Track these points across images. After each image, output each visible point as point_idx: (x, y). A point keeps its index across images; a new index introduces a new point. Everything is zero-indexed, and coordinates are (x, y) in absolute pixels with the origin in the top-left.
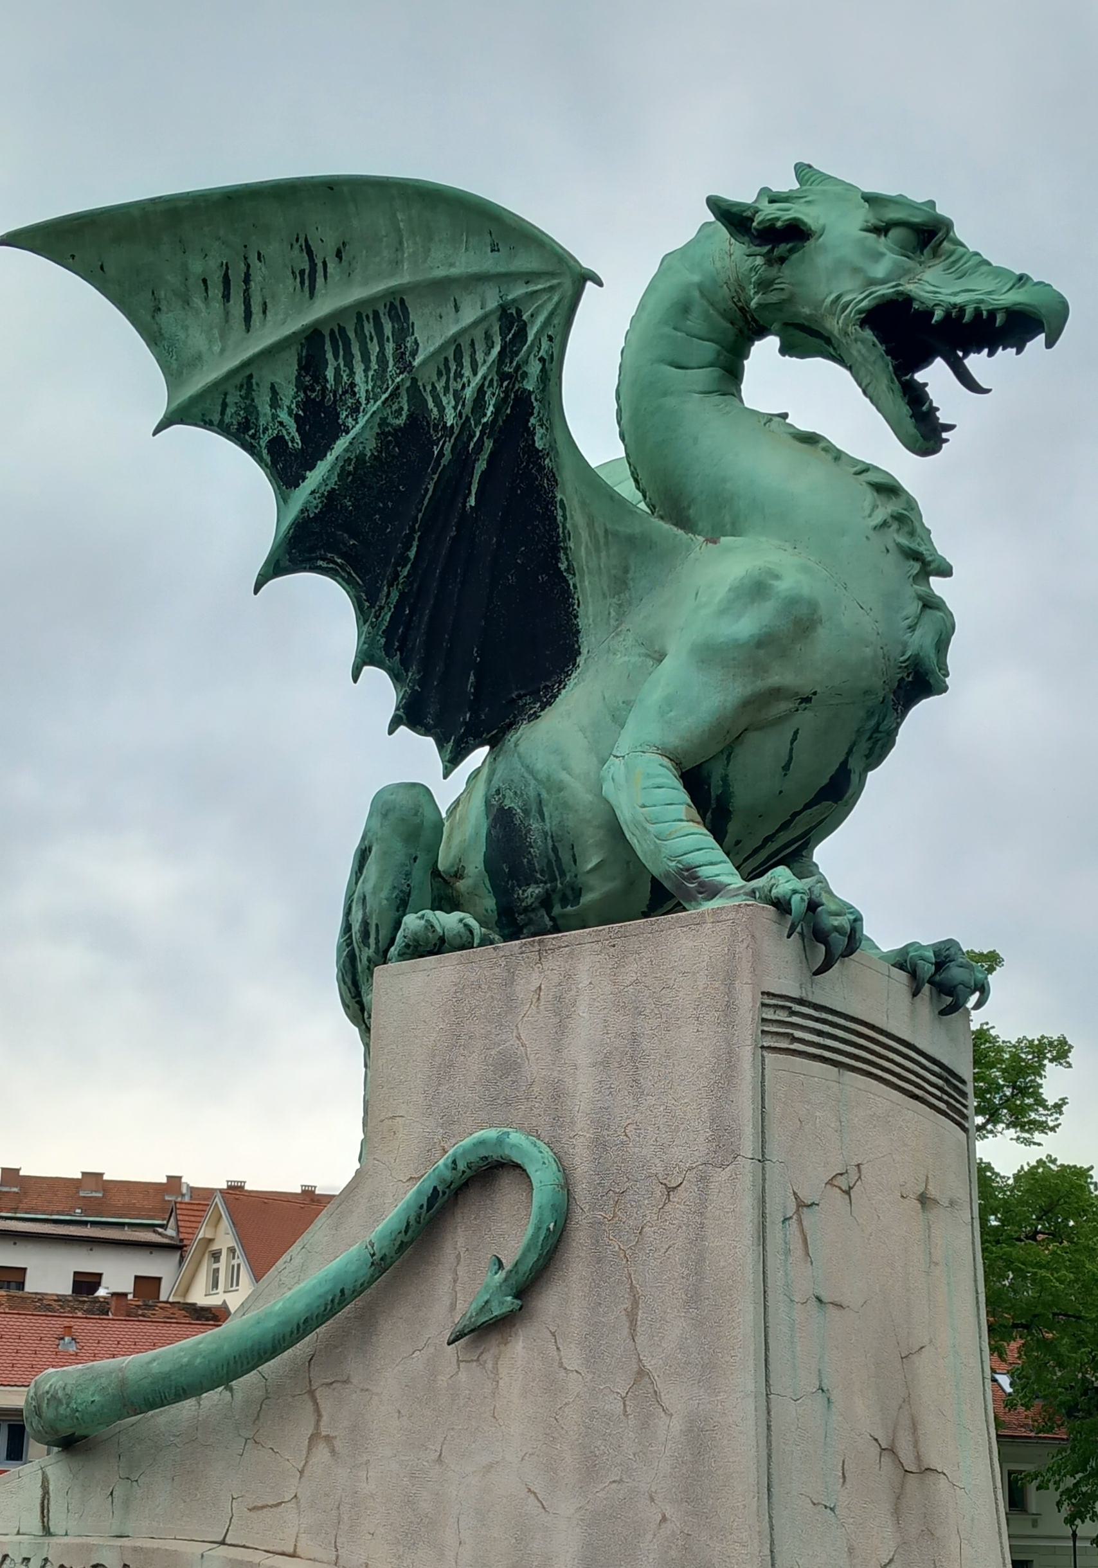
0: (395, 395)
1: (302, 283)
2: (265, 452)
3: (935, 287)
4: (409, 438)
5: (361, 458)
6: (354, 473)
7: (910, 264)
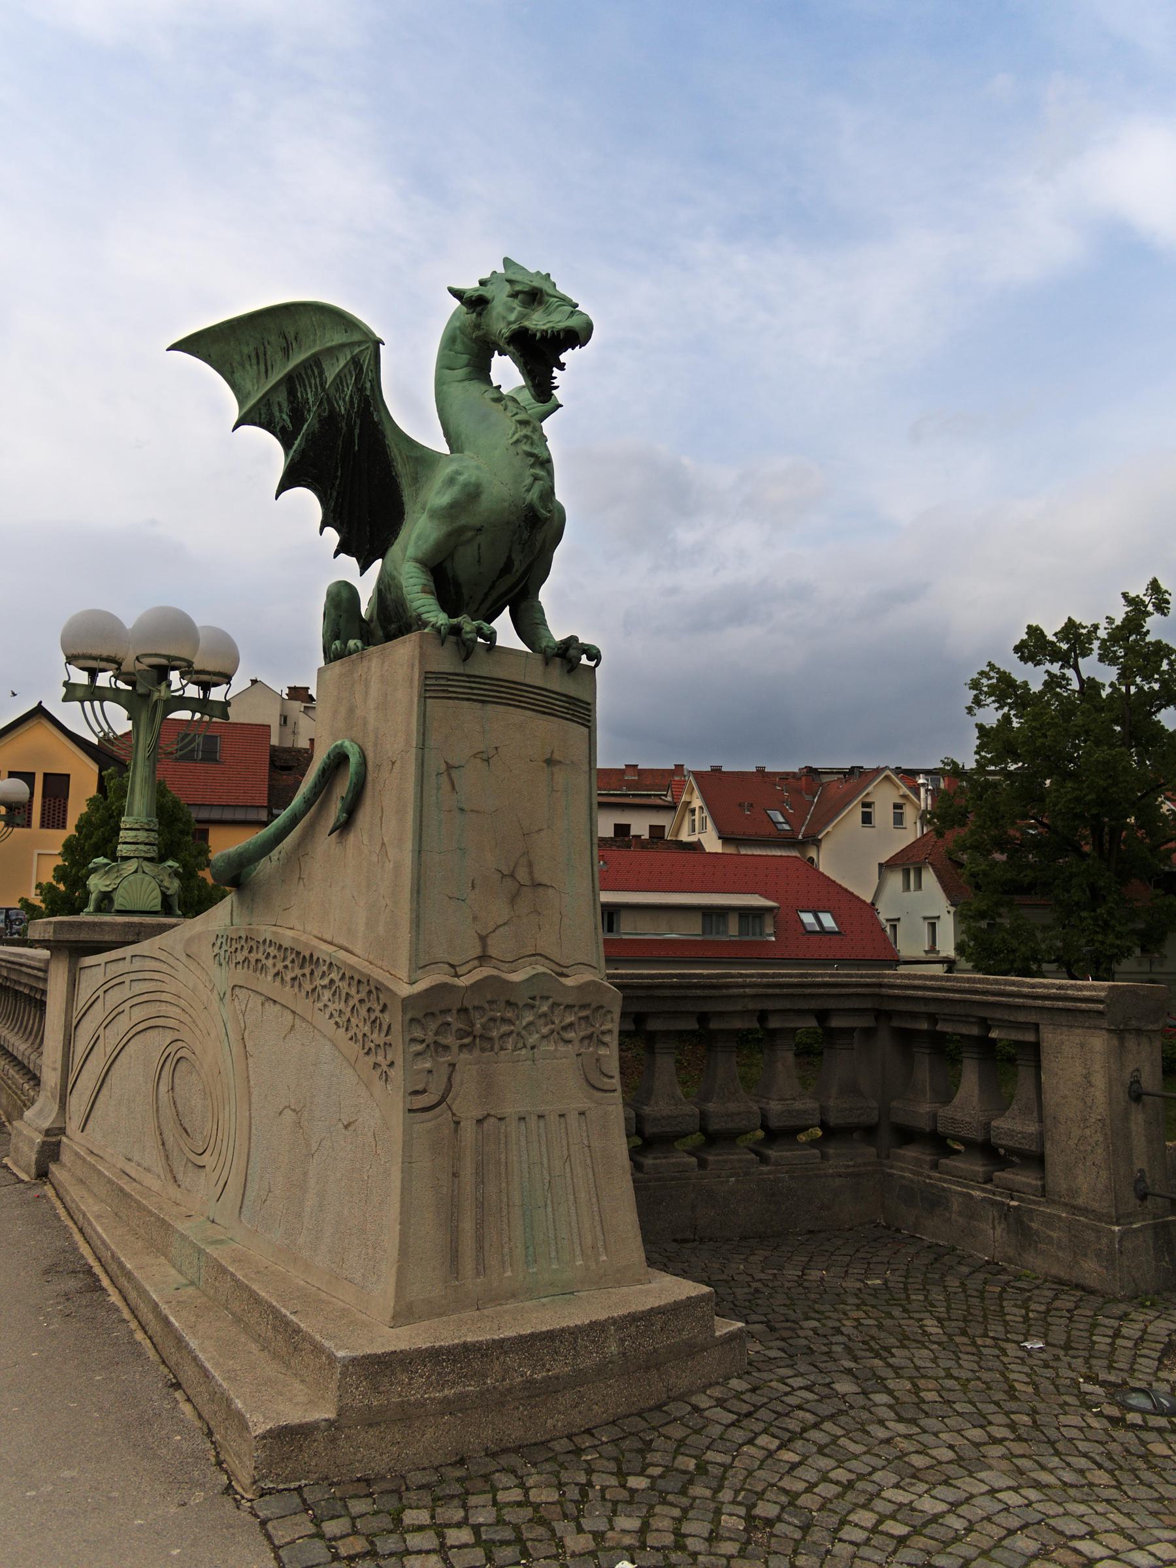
0: (321, 403)
3: (539, 321)
4: (330, 421)
5: (313, 433)
6: (311, 439)
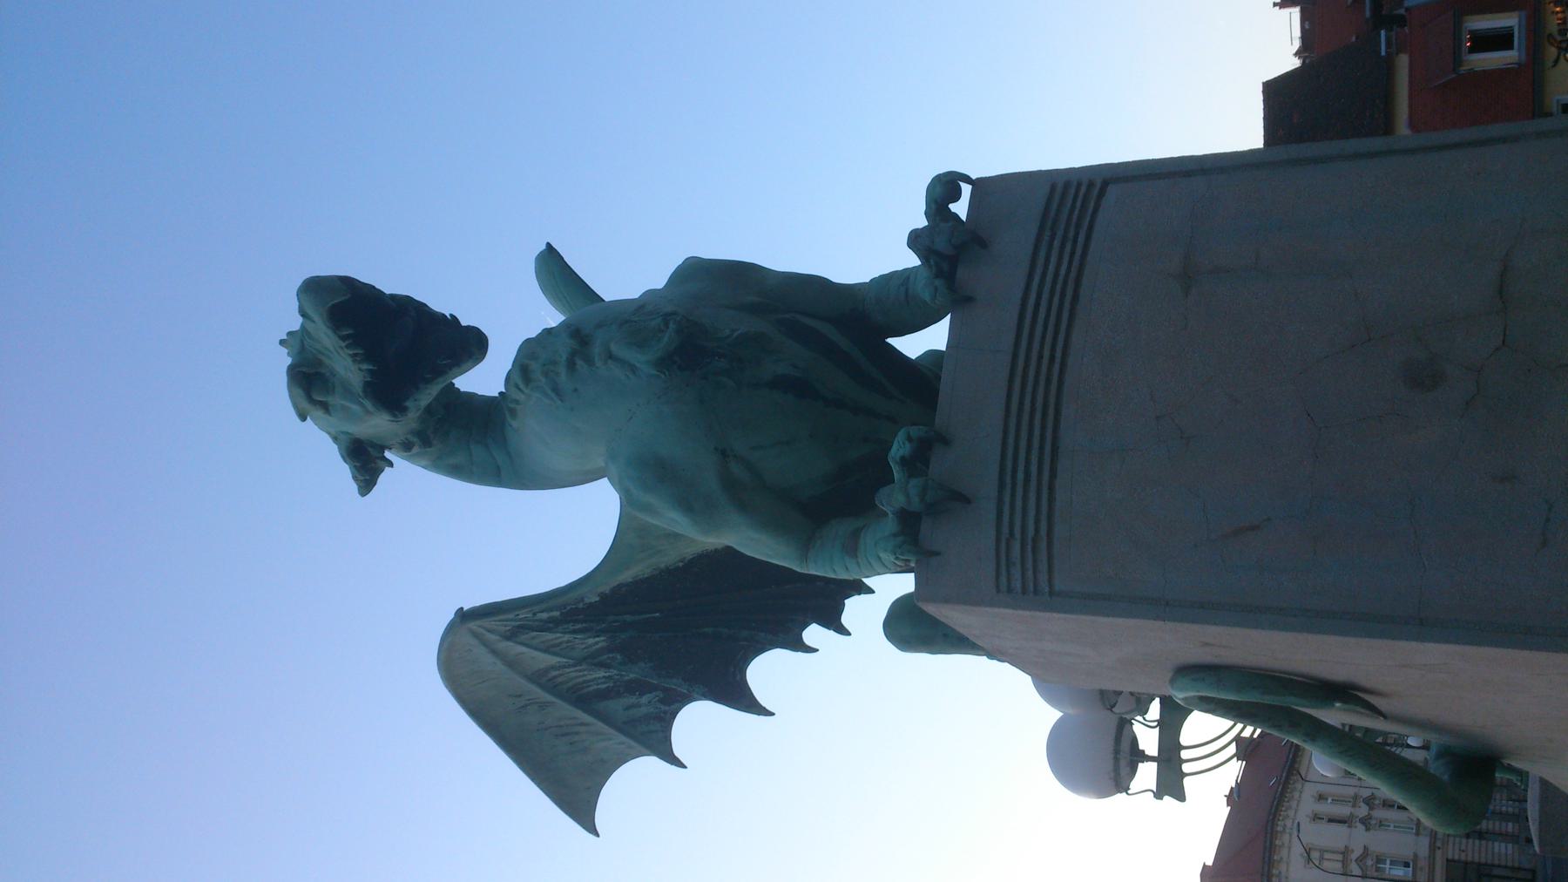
3: (346, 367)
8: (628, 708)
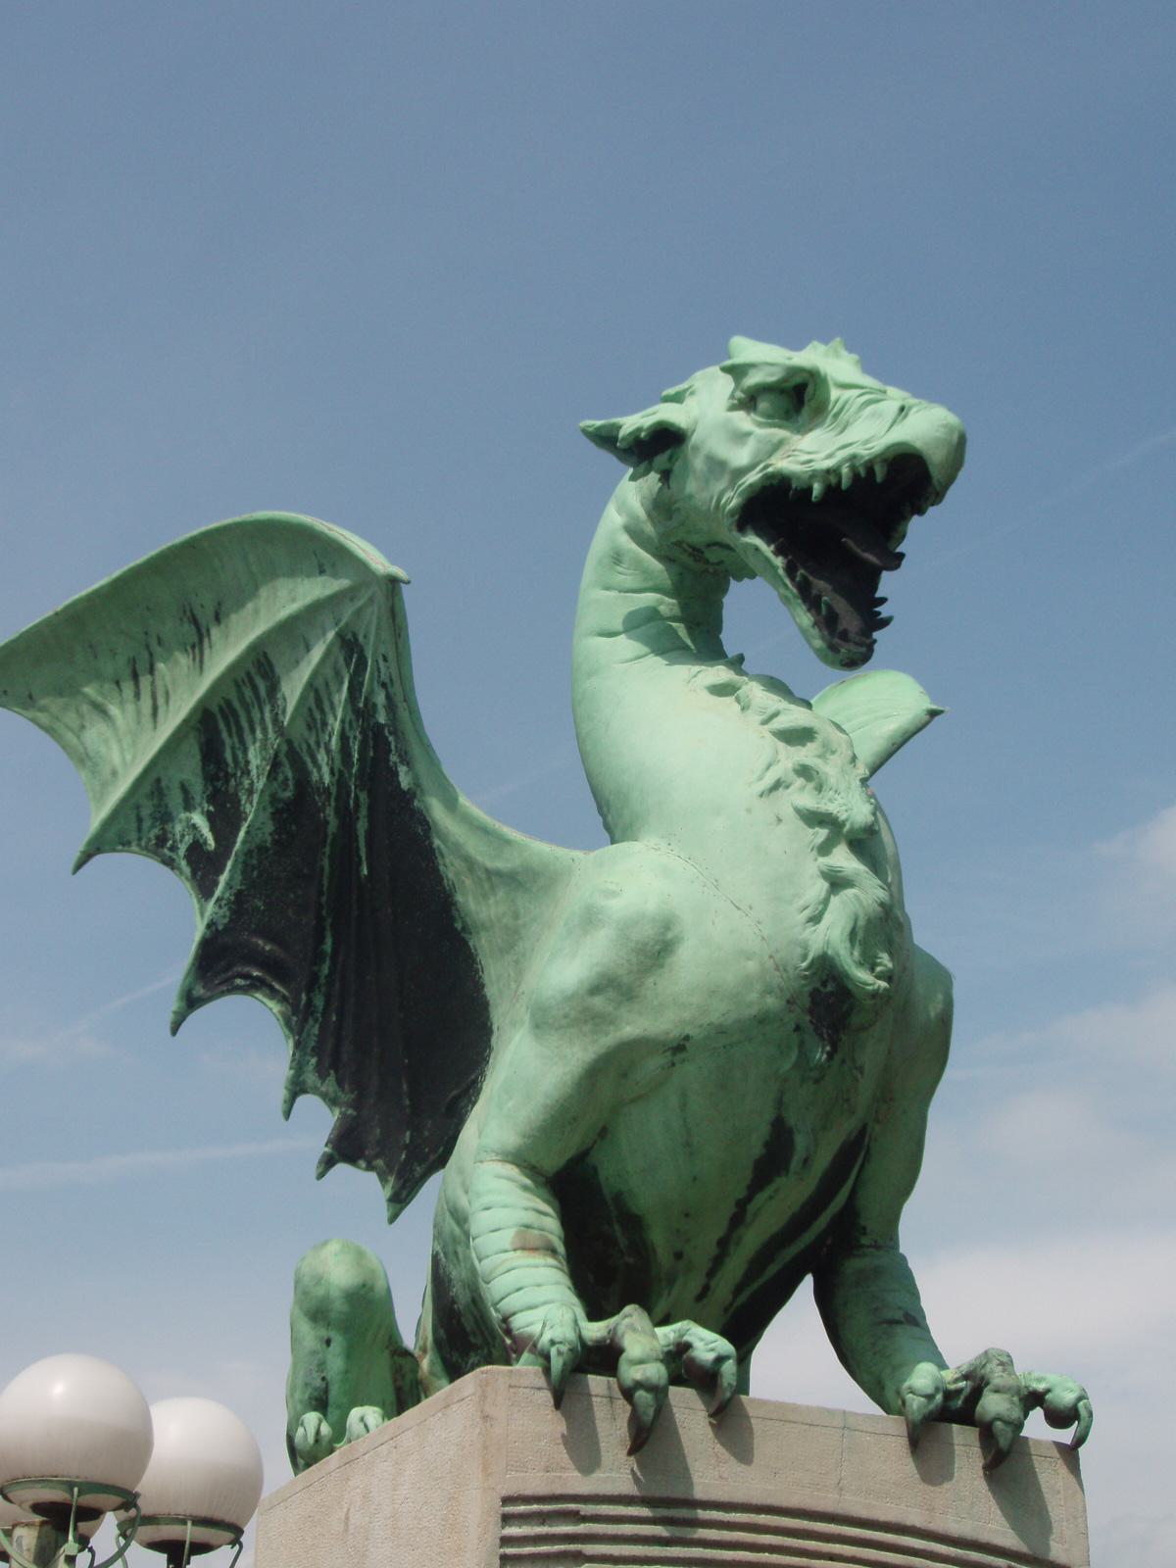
0: (275, 765)
1: (194, 659)
2: (183, 863)
7: (780, 433)
8: (184, 789)
